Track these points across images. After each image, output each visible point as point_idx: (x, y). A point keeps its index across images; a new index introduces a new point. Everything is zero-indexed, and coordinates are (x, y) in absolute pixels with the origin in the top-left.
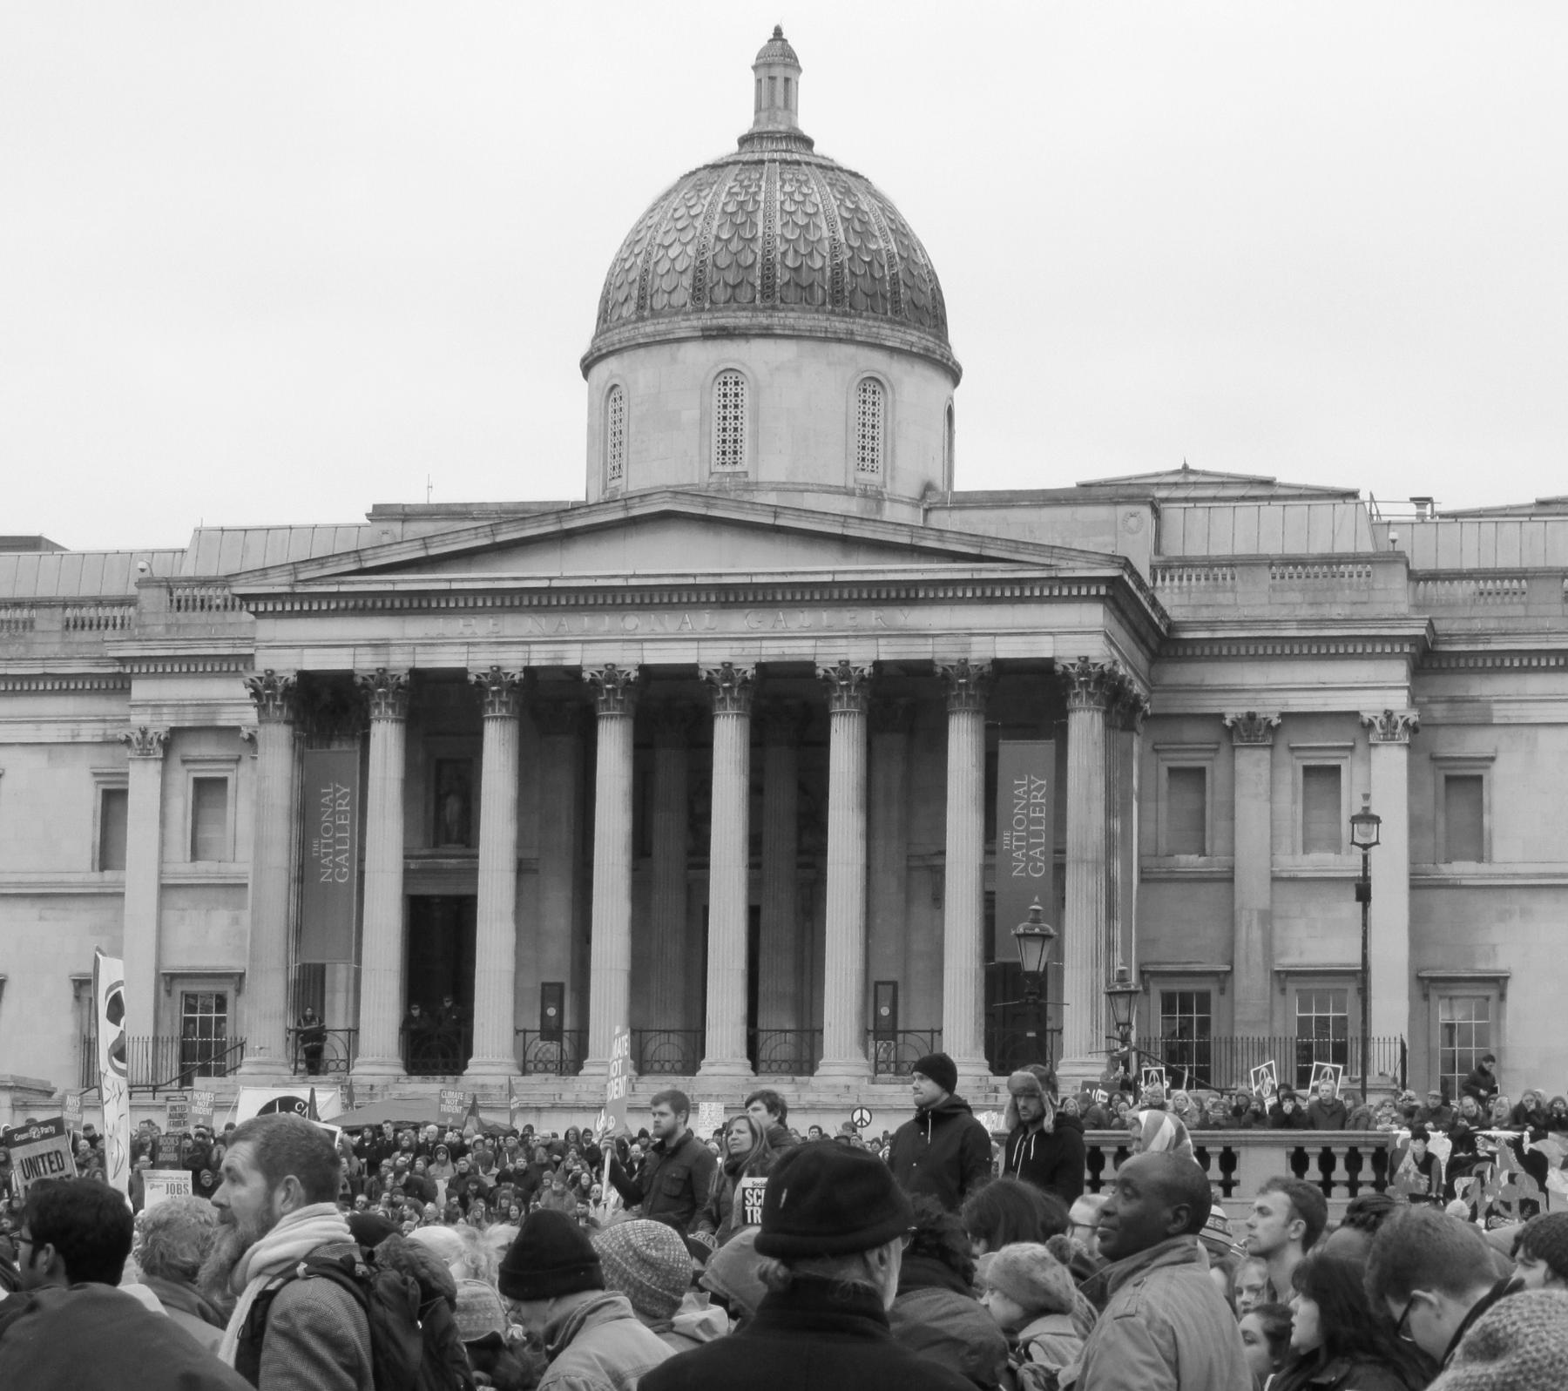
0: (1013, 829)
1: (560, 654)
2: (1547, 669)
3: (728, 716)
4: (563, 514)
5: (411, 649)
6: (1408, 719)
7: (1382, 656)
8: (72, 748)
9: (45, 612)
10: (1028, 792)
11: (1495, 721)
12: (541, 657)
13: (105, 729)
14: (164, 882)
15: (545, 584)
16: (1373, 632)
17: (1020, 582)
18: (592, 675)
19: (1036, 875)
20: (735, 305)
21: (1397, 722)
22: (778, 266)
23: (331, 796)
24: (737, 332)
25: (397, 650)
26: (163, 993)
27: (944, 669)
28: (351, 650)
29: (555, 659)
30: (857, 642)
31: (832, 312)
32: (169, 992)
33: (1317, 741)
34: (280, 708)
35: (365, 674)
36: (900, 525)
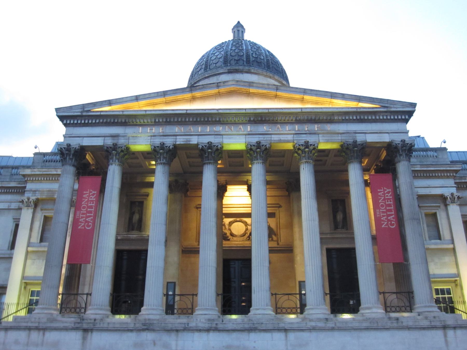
0: (380, 209)
1: (188, 140)
6: (459, 196)
7: (448, 177)
10: (384, 194)
12: (180, 141)
13: (20, 205)
16: (444, 169)
18: (202, 146)
19: (392, 227)
20: (238, 65)
21: (455, 197)
22: (251, 56)
23: (88, 194)
25: (122, 138)
27: (348, 145)
28: (103, 138)
29: (186, 141)
30: (311, 136)
31: (267, 70)
32: (25, 288)
33: (427, 204)
34: (71, 159)
35: (108, 146)
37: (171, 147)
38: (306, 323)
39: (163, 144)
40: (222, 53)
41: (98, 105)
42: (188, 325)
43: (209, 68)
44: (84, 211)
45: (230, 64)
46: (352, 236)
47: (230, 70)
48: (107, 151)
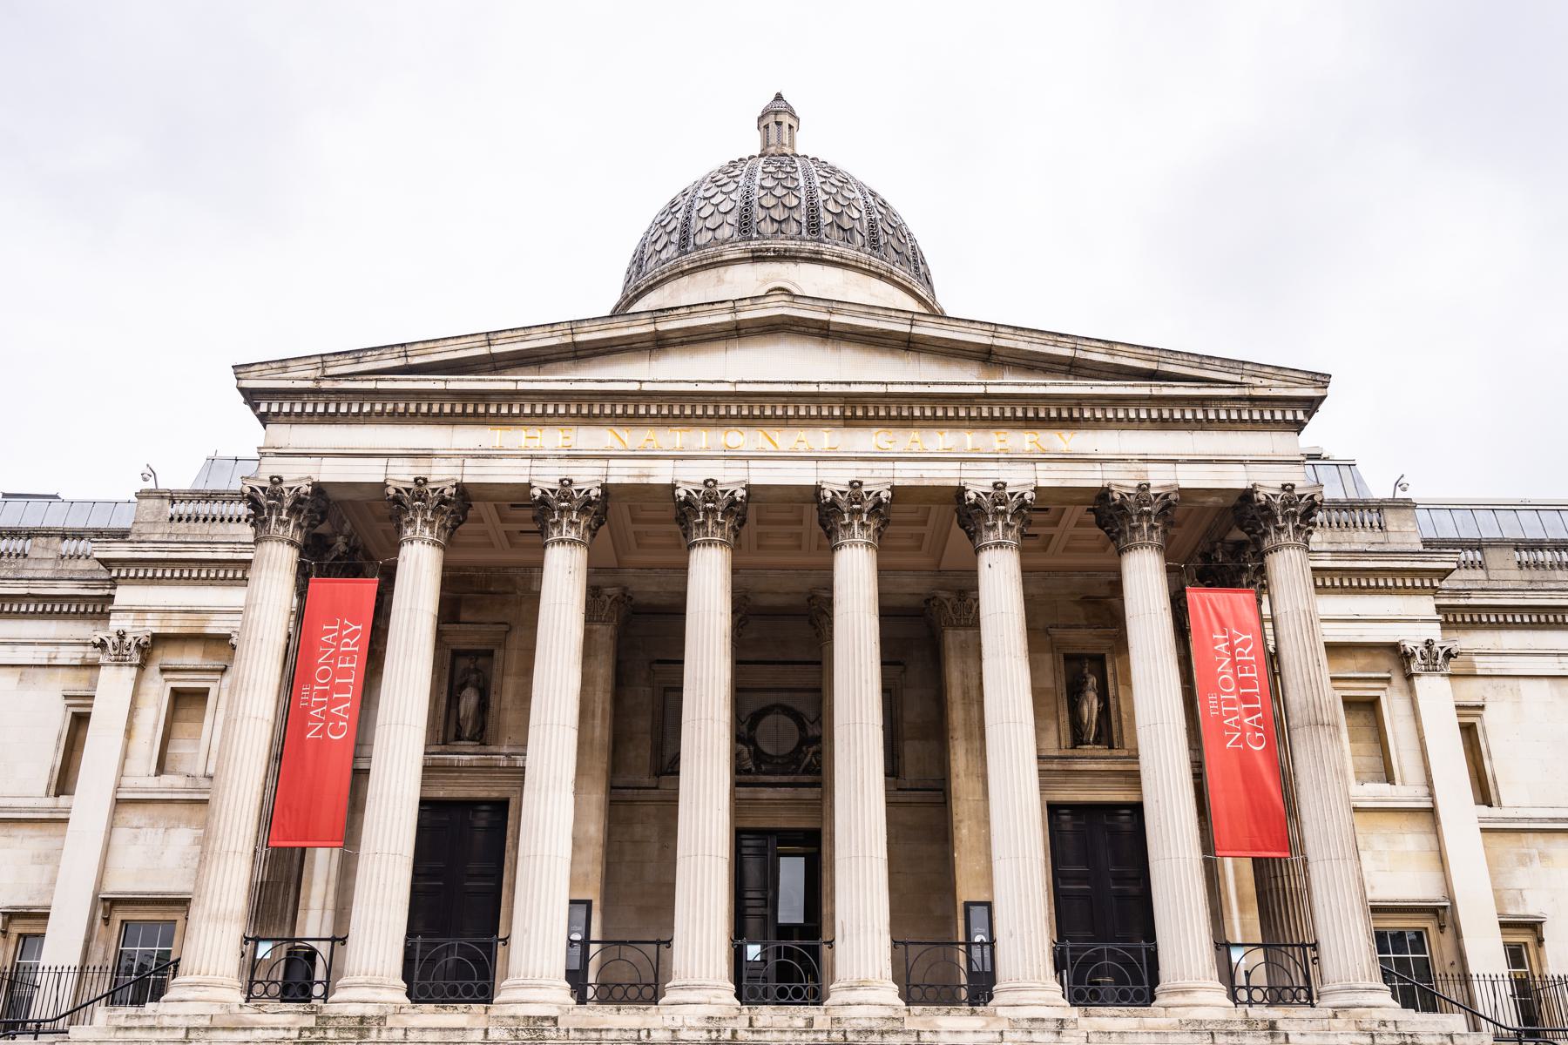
1: (646, 472)
2: (1523, 626)
3: (857, 546)
4: (658, 314)
5: (459, 462)
6: (1449, 650)
8: (47, 670)
9: (42, 541)
11: (1479, 672)
12: (622, 473)
13: (85, 653)
14: (120, 796)
15: (634, 387)
17: (1203, 401)
18: (688, 493)
21: (1437, 653)
22: (822, 210)
24: (787, 254)
25: (444, 462)
26: (99, 921)
28: (384, 461)
32: (106, 921)
35: (400, 486)
36: (1061, 335)
37: (593, 493)
38: (1001, 1033)
39: (566, 483)
40: (733, 196)
41: (369, 359)
42: (649, 1035)
43: (695, 244)
44: (325, 685)
45: (758, 233)
46: (1135, 767)
47: (757, 251)
48: (397, 500)
